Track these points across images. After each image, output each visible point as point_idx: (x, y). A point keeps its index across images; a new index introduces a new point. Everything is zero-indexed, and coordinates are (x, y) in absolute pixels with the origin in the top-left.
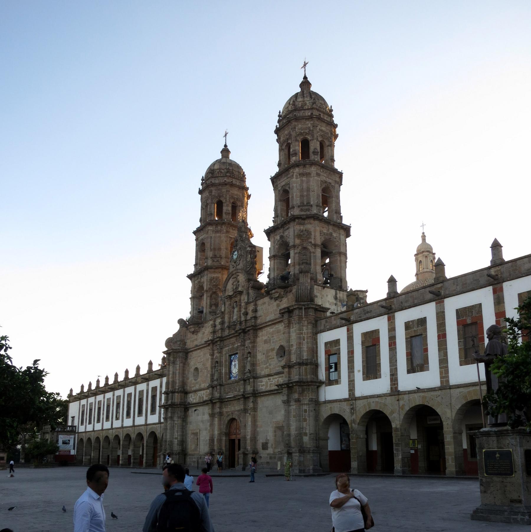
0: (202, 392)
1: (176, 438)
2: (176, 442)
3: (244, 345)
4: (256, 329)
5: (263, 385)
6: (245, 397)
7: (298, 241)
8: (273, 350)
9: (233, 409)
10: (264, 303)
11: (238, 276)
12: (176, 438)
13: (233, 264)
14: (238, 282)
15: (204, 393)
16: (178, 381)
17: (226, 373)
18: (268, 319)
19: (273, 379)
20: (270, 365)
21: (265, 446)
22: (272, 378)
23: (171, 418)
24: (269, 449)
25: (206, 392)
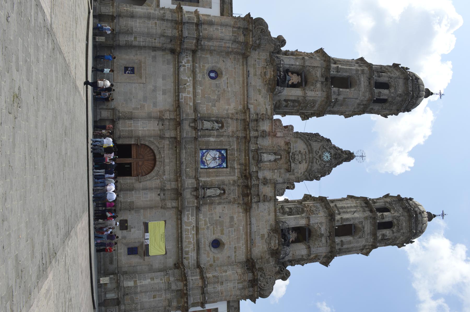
0: (191, 89)
1: (135, 38)
2: (131, 38)
3: (233, 185)
4: (247, 208)
5: (188, 219)
6: (178, 194)
7: (312, 256)
8: (222, 233)
9: (167, 161)
10: (269, 215)
11: (306, 163)
12: (135, 38)
13: (319, 154)
14: (300, 163)
15: (189, 93)
16: (210, 44)
17: (208, 142)
18: (253, 220)
19: (193, 234)
20: (208, 228)
21: (124, 225)
22: (194, 232)
23: (163, 19)
24: (121, 231)
25: (190, 98)
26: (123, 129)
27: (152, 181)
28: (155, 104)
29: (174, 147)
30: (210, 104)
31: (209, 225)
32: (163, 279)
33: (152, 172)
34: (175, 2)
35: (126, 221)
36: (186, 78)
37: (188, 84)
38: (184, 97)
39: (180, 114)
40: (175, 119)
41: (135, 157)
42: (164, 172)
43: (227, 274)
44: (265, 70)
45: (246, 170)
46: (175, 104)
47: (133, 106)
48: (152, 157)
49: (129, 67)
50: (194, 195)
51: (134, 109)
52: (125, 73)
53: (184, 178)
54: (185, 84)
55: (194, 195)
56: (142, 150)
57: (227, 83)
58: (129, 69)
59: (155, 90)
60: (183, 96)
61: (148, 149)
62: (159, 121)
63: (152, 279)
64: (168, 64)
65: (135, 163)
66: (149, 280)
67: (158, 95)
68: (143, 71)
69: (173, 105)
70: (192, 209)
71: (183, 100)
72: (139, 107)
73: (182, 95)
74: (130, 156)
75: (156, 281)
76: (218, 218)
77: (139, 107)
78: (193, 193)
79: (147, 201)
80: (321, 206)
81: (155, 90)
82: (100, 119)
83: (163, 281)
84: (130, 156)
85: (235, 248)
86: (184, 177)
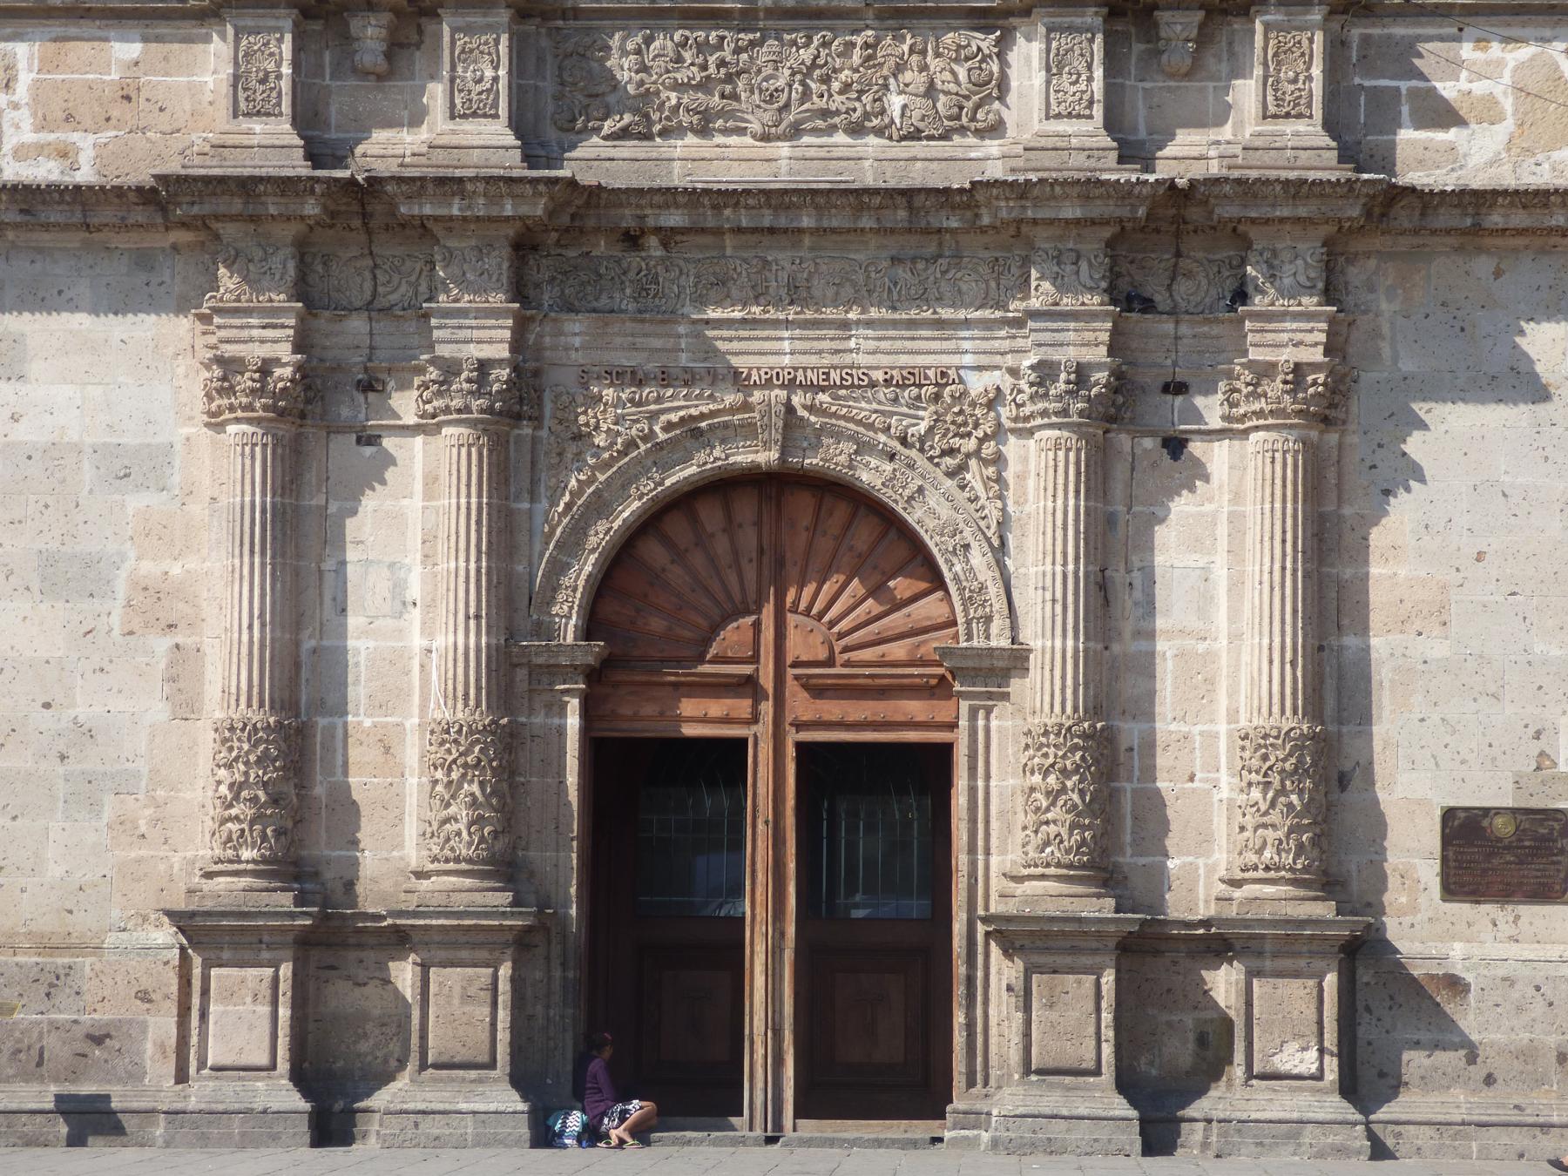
26: (411, 829)
27: (1010, 523)
28: (129, 468)
29: (633, 260)
33: (913, 517)
35: (1464, 833)
38: (43, 125)
39: (247, 186)
40: (303, 250)
41: (743, 707)
42: (912, 378)
46: (122, 241)
47: (158, 711)
48: (746, 507)
50: (1204, 38)
51: (185, 707)
53: (993, 147)
55: (1204, 38)
56: (657, 624)
60: (29, 136)
61: (654, 552)
62: (333, 429)
69: (144, 260)
70: (1367, 63)
71: (86, 145)
72: (162, 645)
73: (20, 153)
74: (725, 761)
77: (162, 645)
78: (1178, 58)
79: (1236, 585)
82: (300, 1078)
84: (725, 761)
86: (989, 159)
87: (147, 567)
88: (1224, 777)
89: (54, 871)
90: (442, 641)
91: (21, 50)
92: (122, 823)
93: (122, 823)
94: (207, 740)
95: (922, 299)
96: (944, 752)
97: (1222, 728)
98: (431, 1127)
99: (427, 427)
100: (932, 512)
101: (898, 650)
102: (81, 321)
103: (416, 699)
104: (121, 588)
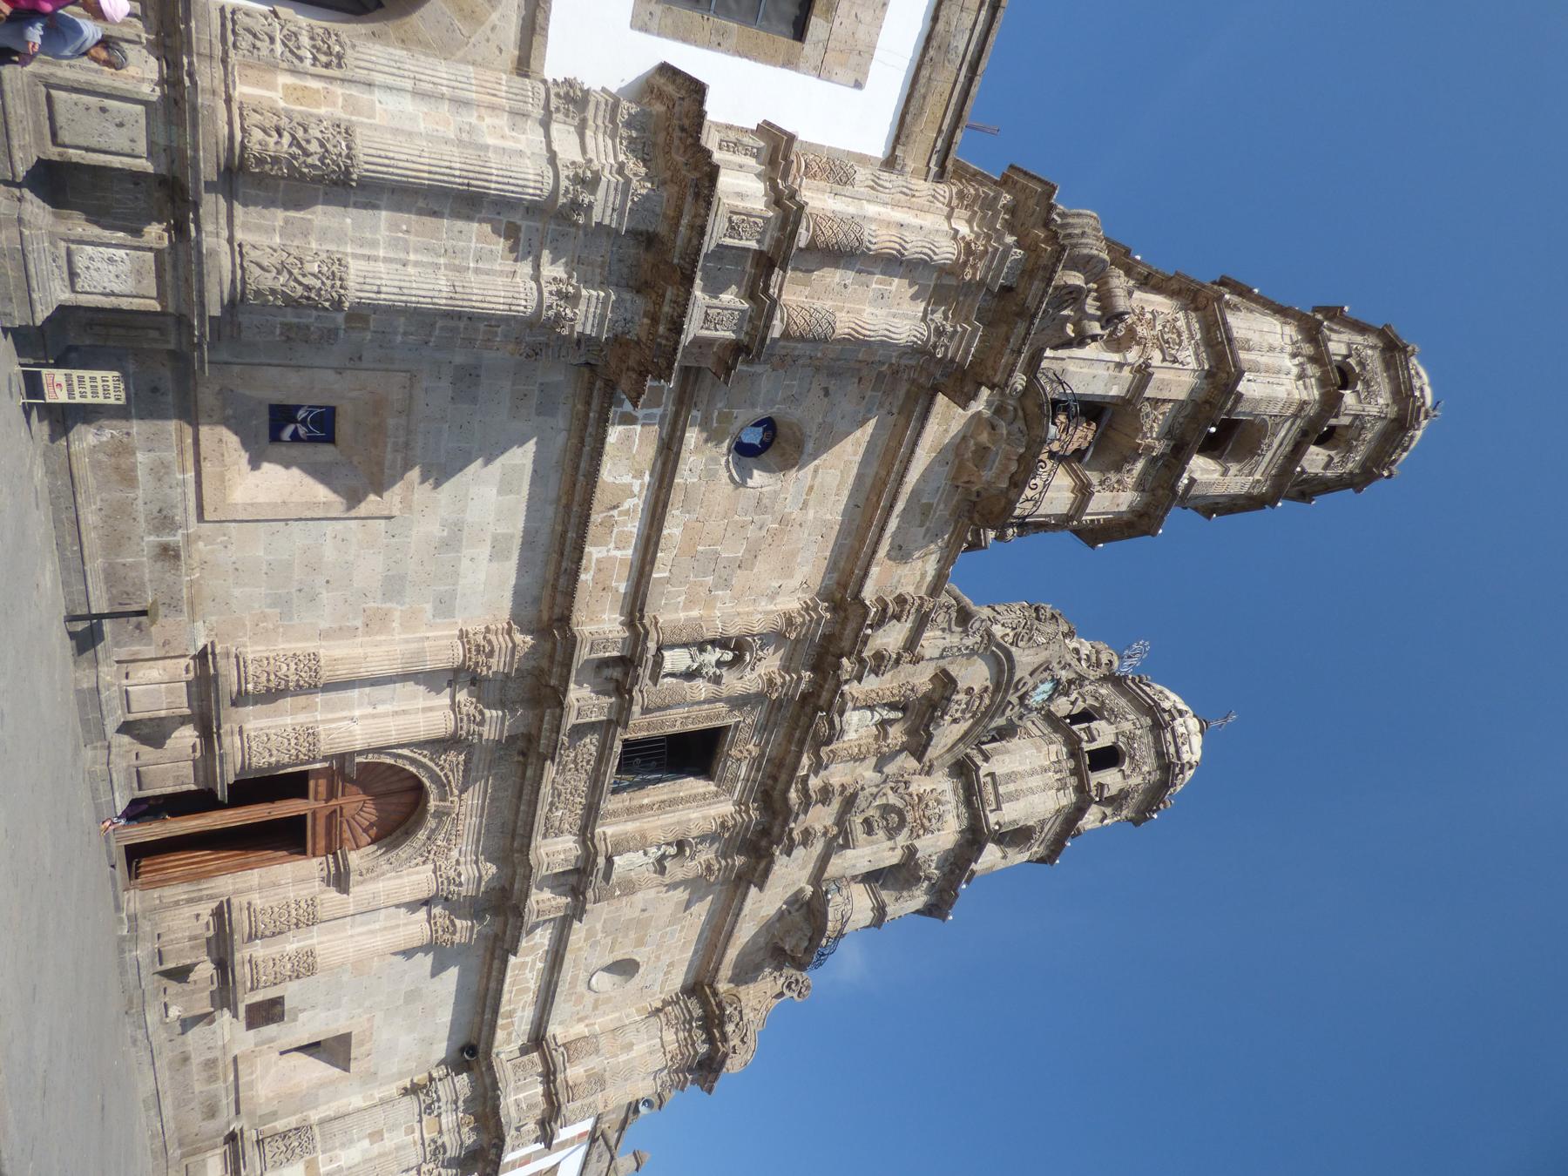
28: (444, 606)
30: (710, 579)
31: (600, 935)
32: (417, 1126)
34: (658, 9)
36: (627, 479)
37: (628, 504)
43: (633, 1054)
44: (984, 437)
45: (775, 779)
47: (323, 625)
49: (298, 407)
52: (275, 437)
54: (615, 507)
57: (811, 488)
58: (301, 414)
59: (451, 542)
60: (595, 557)
63: (376, 1136)
64: (545, 408)
65: (321, 823)
66: (366, 1143)
67: (465, 563)
68: (389, 456)
69: (537, 600)
75: (390, 1141)
76: (637, 913)
77: (359, 623)
80: (955, 792)
81: (451, 542)
83: (417, 1135)
85: (671, 965)
87: (397, 614)
88: (295, 946)
89: (237, 592)
90: (357, 729)
91: (629, 552)
92: (265, 617)
93: (265, 617)
94: (310, 646)
95: (488, 831)
96: (303, 852)
97: (315, 941)
98: (103, 787)
99: (454, 706)
100: (404, 851)
101: (347, 834)
102: (513, 581)
103: (330, 716)
104: (388, 605)
